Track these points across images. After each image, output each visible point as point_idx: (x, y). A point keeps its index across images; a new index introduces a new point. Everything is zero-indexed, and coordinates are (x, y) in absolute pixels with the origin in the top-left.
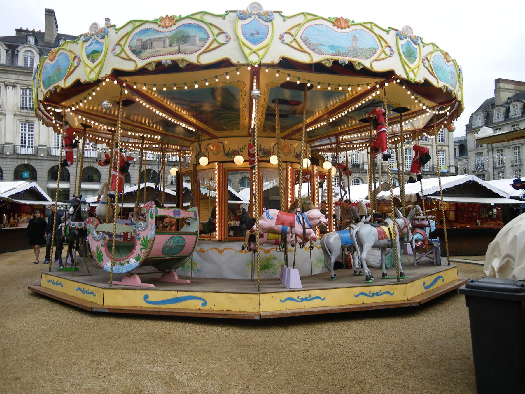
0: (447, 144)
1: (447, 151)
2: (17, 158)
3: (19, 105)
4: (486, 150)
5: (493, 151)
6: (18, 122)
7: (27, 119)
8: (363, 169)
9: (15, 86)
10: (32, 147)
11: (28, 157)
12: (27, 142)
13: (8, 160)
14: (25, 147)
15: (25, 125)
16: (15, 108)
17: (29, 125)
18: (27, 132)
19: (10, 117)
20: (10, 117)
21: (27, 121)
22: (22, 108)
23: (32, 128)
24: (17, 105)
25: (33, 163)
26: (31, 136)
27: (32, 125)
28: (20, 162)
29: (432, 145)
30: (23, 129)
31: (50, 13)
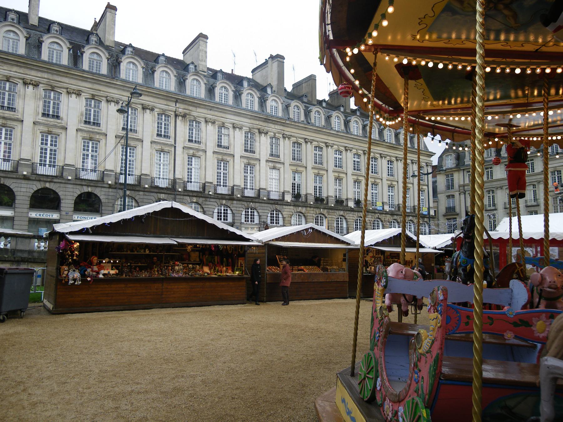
0: (381, 177)
1: (396, 187)
4: (457, 193)
5: (465, 194)
8: (347, 206)
23: (11, 135)
26: (54, 153)
27: (11, 131)
29: (413, 184)
30: (44, 142)
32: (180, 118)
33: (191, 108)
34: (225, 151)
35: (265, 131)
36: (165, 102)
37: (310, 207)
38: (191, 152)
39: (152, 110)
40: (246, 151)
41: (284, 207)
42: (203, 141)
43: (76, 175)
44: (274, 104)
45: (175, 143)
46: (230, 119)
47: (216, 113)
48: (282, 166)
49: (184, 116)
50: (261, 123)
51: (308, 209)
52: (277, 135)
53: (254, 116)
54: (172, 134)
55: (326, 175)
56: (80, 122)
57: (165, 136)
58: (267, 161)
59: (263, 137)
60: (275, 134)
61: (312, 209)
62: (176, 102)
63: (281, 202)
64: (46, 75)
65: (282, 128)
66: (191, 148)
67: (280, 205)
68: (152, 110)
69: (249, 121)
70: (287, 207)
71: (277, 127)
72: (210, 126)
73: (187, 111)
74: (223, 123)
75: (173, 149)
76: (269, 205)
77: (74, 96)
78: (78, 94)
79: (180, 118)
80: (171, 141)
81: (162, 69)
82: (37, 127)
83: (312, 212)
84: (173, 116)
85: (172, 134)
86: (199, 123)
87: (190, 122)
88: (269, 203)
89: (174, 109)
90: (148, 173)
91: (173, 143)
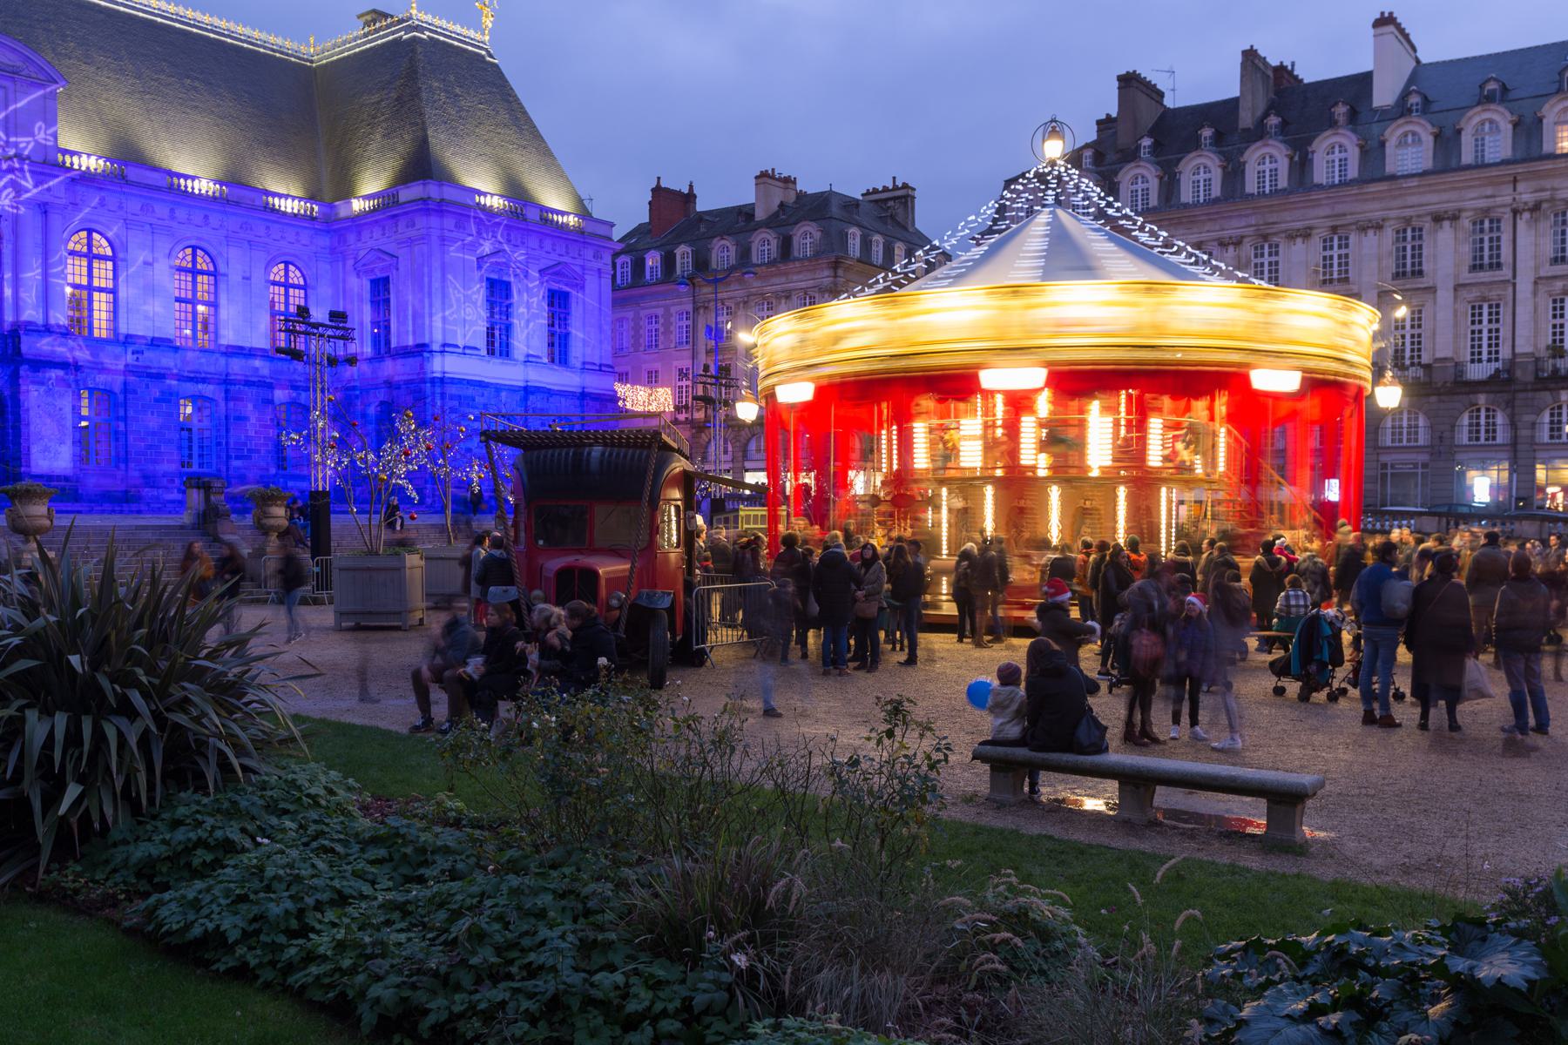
15: (1481, 307)
17: (1490, 307)
18: (1485, 326)
22: (1476, 267)
31: (691, 186)
32: (1526, 215)
36: (1489, 191)
39: (1455, 218)
45: (1514, 277)
49: (1536, 208)
57: (1491, 265)
62: (1515, 181)
66: (1555, 277)
68: (1455, 218)
73: (1546, 195)
75: (1510, 289)
77: (1299, 240)
78: (1306, 234)
79: (1526, 215)
82: (1464, 293)
84: (1508, 216)
87: (1556, 215)
89: (1508, 199)
90: (1449, 354)
91: (1509, 276)
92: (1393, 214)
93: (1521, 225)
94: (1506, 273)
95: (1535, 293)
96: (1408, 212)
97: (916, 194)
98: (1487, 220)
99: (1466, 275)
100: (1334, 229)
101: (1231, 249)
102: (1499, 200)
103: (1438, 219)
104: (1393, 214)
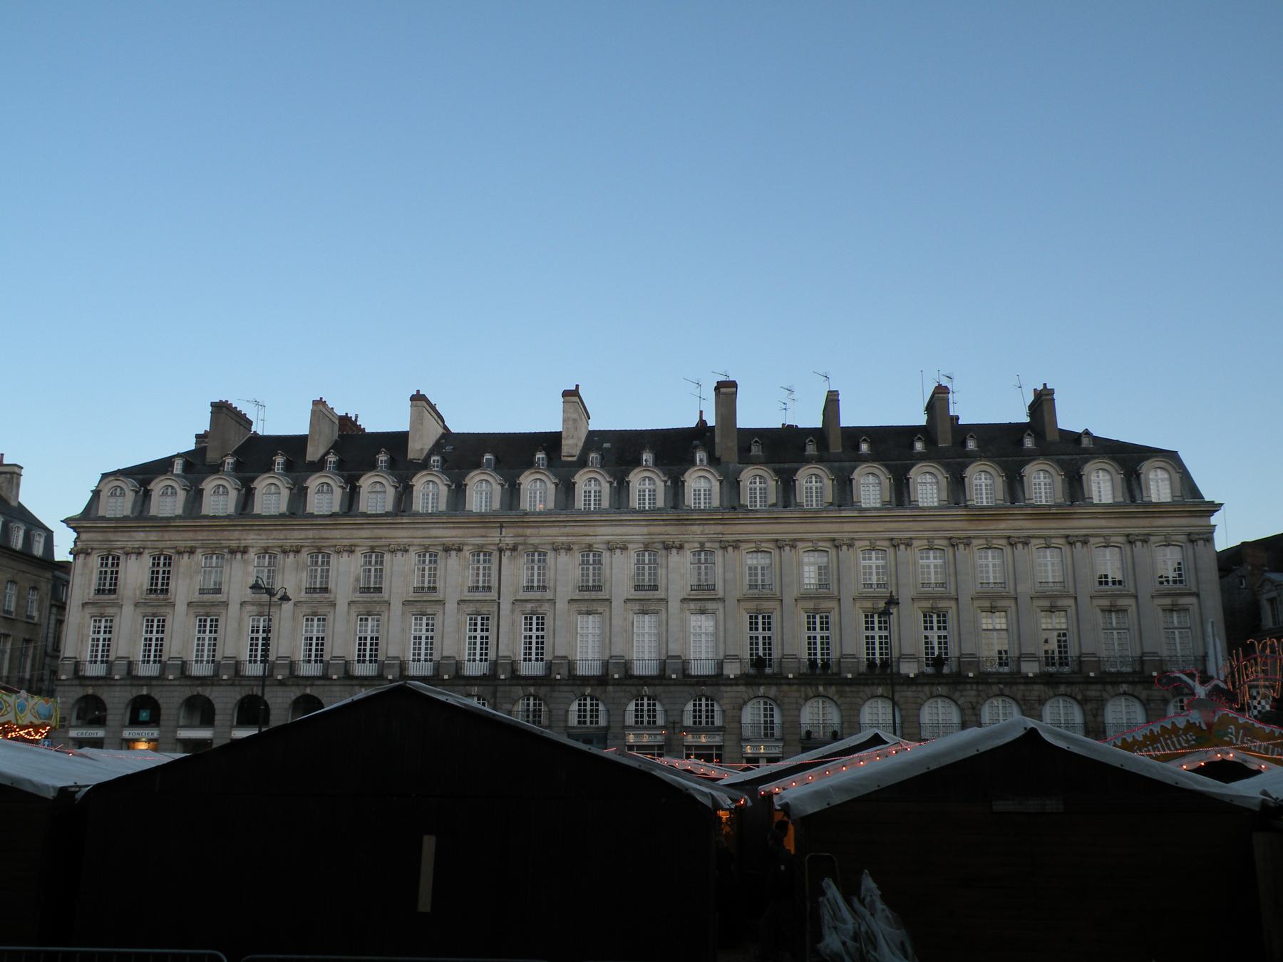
2: (132, 685)
3: (146, 586)
6: (140, 617)
7: (208, 610)
9: (140, 553)
10: (321, 661)
11: (202, 680)
12: (368, 653)
13: (118, 689)
14: (364, 662)
16: (138, 592)
19: (128, 609)
20: (128, 609)
21: (154, 615)
24: (142, 585)
25: (156, 694)
28: (135, 692)
32: (508, 553)
33: (528, 531)
34: (594, 595)
35: (677, 544)
36: (482, 531)
37: (789, 684)
38: (529, 606)
40: (638, 588)
41: (723, 688)
42: (552, 584)
43: (626, 671)
44: (703, 485)
46: (605, 533)
47: (577, 530)
48: (720, 606)
49: (514, 549)
50: (669, 529)
51: (785, 688)
52: (708, 545)
53: (649, 516)
54: (494, 583)
55: (837, 610)
56: (354, 590)
58: (684, 600)
59: (674, 557)
60: (702, 545)
61: (795, 687)
62: (501, 527)
63: (718, 679)
64: (311, 534)
65: (719, 528)
66: (526, 601)
67: (713, 685)
69: (645, 530)
70: (729, 689)
71: (707, 529)
72: (563, 558)
73: (520, 539)
74: (590, 546)
76: (687, 689)
77: (345, 555)
79: (508, 553)
80: (493, 595)
81: (477, 478)
83: (797, 694)
84: (496, 554)
85: (494, 583)
86: (545, 554)
88: (685, 685)
91: (496, 597)
92: (416, 541)
93: (504, 560)
94: (493, 595)
95: (513, 611)
96: (427, 542)
97: (23, 472)
98: (479, 550)
99: (466, 593)
100: (372, 549)
101: (292, 555)
102: (490, 540)
103: (447, 549)
104: (416, 541)
